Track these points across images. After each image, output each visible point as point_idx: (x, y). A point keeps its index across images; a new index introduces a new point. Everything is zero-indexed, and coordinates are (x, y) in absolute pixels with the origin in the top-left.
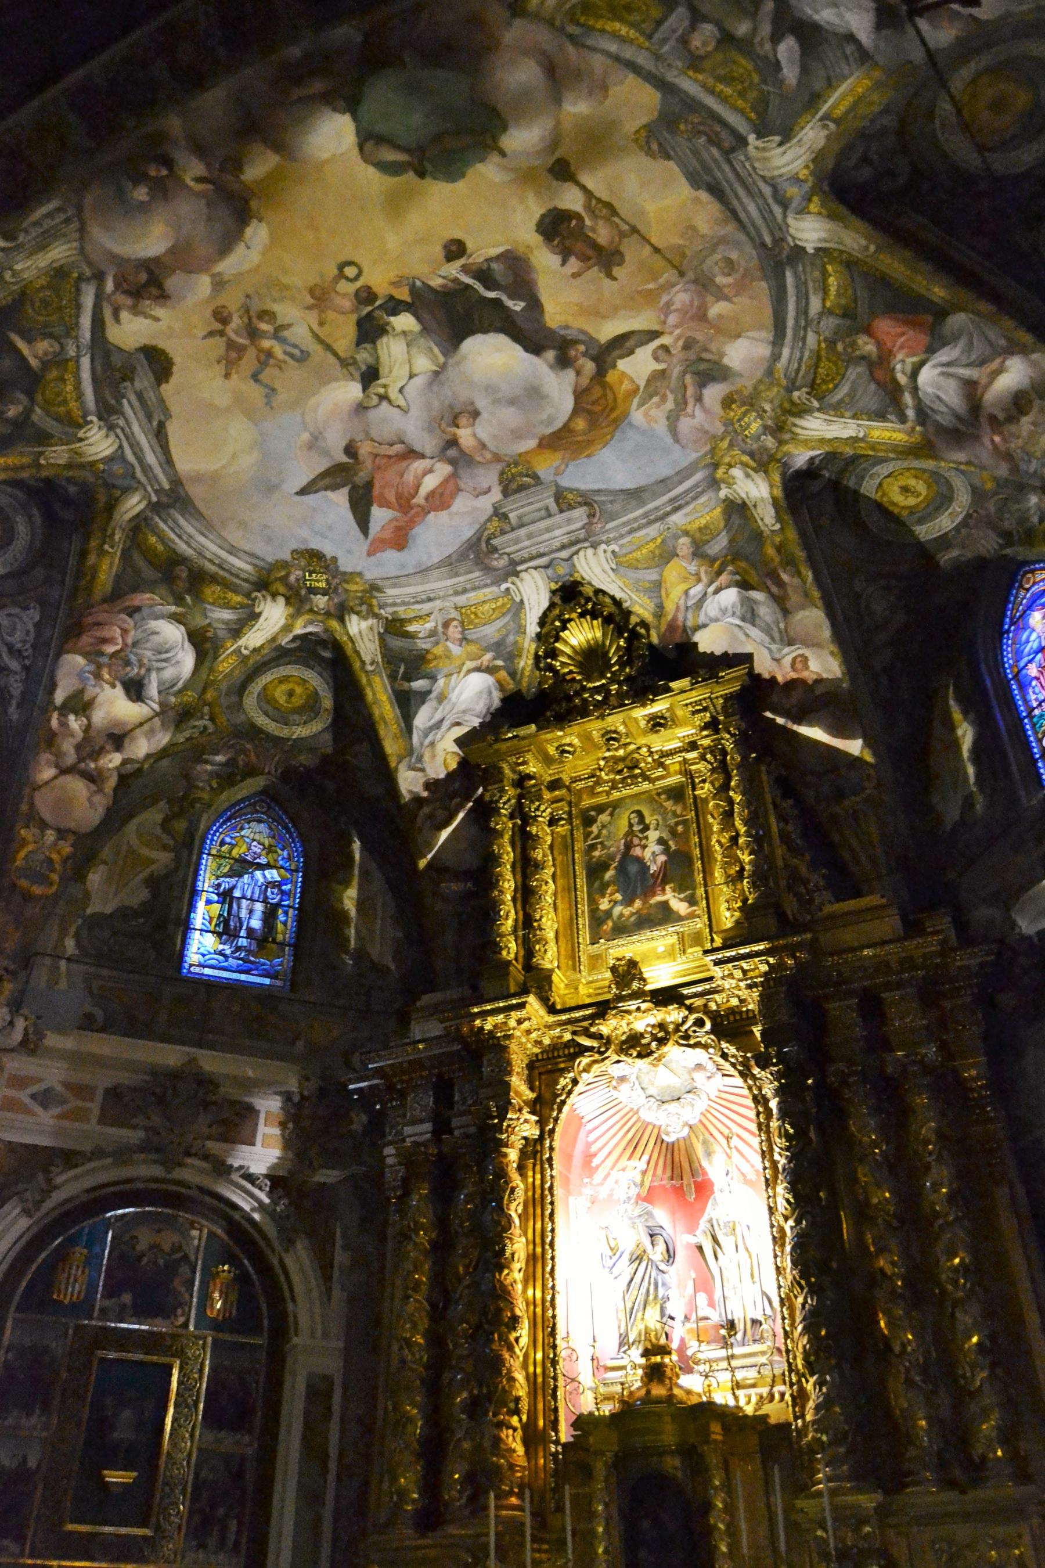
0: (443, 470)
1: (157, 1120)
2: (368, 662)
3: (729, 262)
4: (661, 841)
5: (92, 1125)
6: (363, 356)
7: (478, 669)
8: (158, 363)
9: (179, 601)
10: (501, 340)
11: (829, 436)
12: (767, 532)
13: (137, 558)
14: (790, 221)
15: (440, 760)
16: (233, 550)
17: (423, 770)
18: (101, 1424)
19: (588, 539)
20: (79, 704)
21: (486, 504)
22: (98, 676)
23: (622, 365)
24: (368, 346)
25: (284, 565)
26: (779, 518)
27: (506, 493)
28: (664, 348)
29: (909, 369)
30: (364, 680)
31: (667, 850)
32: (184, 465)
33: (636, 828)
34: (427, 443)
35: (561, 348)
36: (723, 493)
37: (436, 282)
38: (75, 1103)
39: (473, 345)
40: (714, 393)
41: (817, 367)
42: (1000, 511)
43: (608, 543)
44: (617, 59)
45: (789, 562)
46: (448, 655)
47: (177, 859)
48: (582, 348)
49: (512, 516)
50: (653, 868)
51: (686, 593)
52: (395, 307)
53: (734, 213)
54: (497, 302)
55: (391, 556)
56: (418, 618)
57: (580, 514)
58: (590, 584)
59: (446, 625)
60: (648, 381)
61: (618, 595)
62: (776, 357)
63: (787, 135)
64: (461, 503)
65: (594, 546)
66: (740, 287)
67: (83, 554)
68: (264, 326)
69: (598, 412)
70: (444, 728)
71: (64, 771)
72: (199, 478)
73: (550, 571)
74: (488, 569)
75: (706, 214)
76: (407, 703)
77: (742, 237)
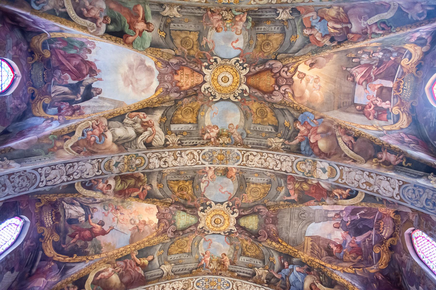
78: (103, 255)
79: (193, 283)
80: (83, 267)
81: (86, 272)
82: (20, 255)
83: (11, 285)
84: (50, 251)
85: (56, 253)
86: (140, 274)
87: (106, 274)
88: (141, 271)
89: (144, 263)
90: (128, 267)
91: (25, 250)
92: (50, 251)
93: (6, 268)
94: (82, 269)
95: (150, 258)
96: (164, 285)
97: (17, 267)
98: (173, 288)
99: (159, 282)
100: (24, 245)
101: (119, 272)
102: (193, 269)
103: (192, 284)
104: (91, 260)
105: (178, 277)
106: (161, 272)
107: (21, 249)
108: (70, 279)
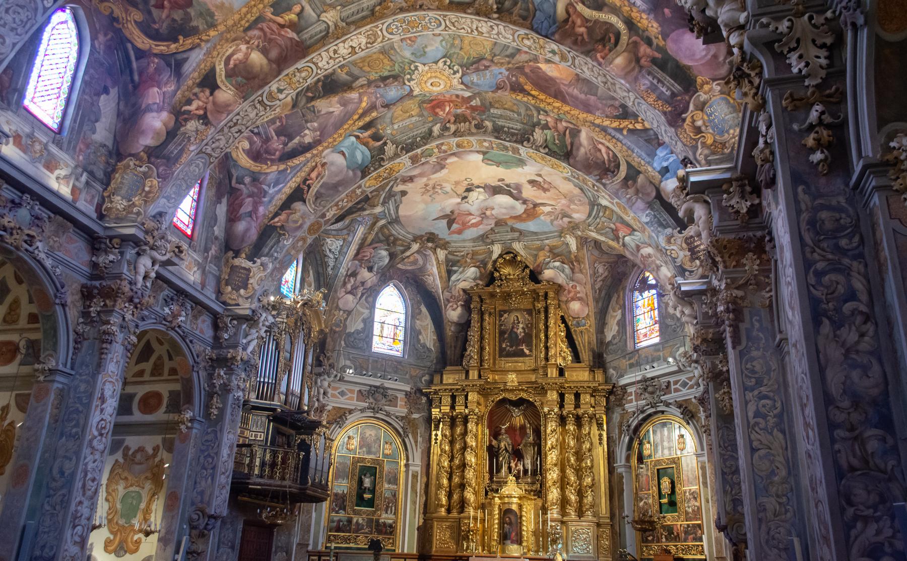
1: (371, 400)
4: (523, 328)
5: (355, 402)
6: (466, 194)
8: (404, 193)
9: (389, 245)
13: (380, 235)
16: (409, 233)
18: (361, 482)
20: (354, 274)
21: (489, 227)
22: (361, 266)
25: (422, 236)
32: (401, 212)
34: (477, 213)
35: (525, 202)
38: (350, 395)
39: (497, 196)
40: (566, 220)
45: (578, 261)
46: (466, 262)
47: (371, 312)
52: (478, 187)
57: (517, 234)
62: (587, 219)
64: (481, 227)
66: (581, 205)
71: (347, 293)
72: (405, 216)
74: (484, 242)
75: (577, 191)
76: (450, 273)
78: (221, 28)
79: (381, 30)
80: (201, 56)
81: (208, 64)
82: (102, 64)
83: (118, 109)
84: (142, 42)
85: (151, 41)
86: (291, 39)
87: (239, 56)
88: (291, 34)
89: (290, 21)
90: (268, 34)
91: (104, 52)
92: (142, 42)
93: (95, 95)
94: (201, 60)
95: (297, 9)
96: (335, 48)
97: (109, 83)
98: (351, 47)
99: (324, 45)
100: (97, 46)
101: (258, 46)
102: (375, 6)
103: (379, 33)
104: (207, 41)
105: (353, 27)
106: (323, 26)
107: (96, 55)
108: (190, 82)
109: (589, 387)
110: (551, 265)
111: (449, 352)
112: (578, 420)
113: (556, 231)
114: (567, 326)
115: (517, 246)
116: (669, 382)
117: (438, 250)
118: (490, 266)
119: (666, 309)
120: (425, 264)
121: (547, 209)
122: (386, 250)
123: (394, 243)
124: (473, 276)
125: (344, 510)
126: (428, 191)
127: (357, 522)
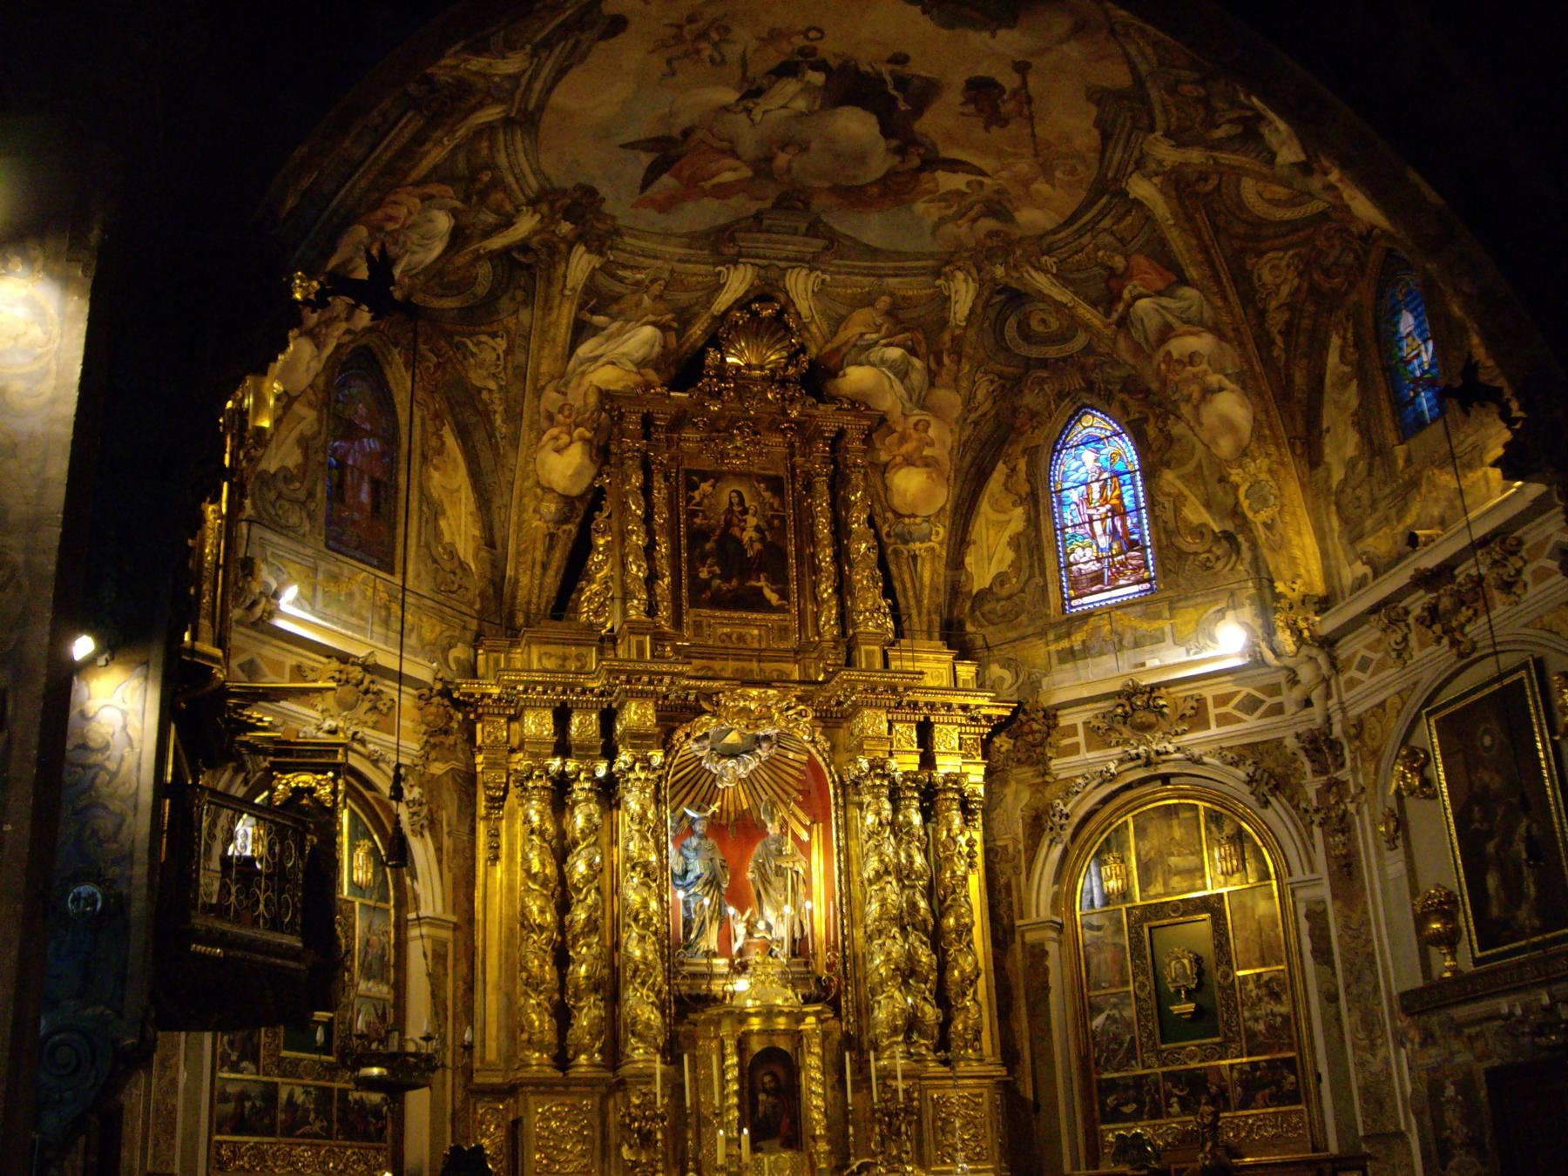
0: (747, 173)
2: (569, 285)
3: (1073, 171)
4: (757, 529)
7: (654, 324)
9: (466, 199)
10: (873, 119)
11: (1046, 291)
12: (953, 322)
13: (461, 158)
14: (1134, 176)
15: (582, 390)
17: (565, 394)
19: (812, 263)
23: (940, 174)
24: (774, 78)
25: (564, 192)
26: (968, 319)
27: (776, 206)
28: (981, 184)
29: (1135, 292)
30: (557, 302)
31: (762, 540)
32: (558, 98)
33: (736, 508)
36: (938, 282)
37: (865, 68)
40: (989, 224)
41: (1076, 253)
42: (1095, 366)
43: (824, 272)
44: (1127, 55)
45: (958, 354)
46: (638, 305)
48: (922, 151)
49: (766, 222)
50: (750, 554)
51: (862, 335)
53: (1103, 151)
54: (895, 99)
55: (651, 214)
56: (632, 268)
57: (818, 244)
58: (787, 293)
59: (653, 281)
60: (950, 192)
61: (804, 312)
62: (1054, 232)
63: (1181, 144)
65: (811, 270)
67: (419, 140)
68: (715, 36)
69: (895, 189)
70: (600, 363)
73: (762, 272)
74: (716, 251)
76: (581, 331)
77: (1096, 165)
109: (965, 708)
110: (875, 354)
111: (524, 580)
112: (930, 797)
113: (931, 256)
114: (877, 536)
115: (800, 287)
116: (1201, 701)
117: (580, 250)
118: (697, 331)
119: (1177, 511)
120: (492, 297)
121: (958, 181)
122: (454, 213)
123: (484, 194)
124: (638, 355)
125: (255, 1059)
126: (679, 38)
127: (291, 1096)
